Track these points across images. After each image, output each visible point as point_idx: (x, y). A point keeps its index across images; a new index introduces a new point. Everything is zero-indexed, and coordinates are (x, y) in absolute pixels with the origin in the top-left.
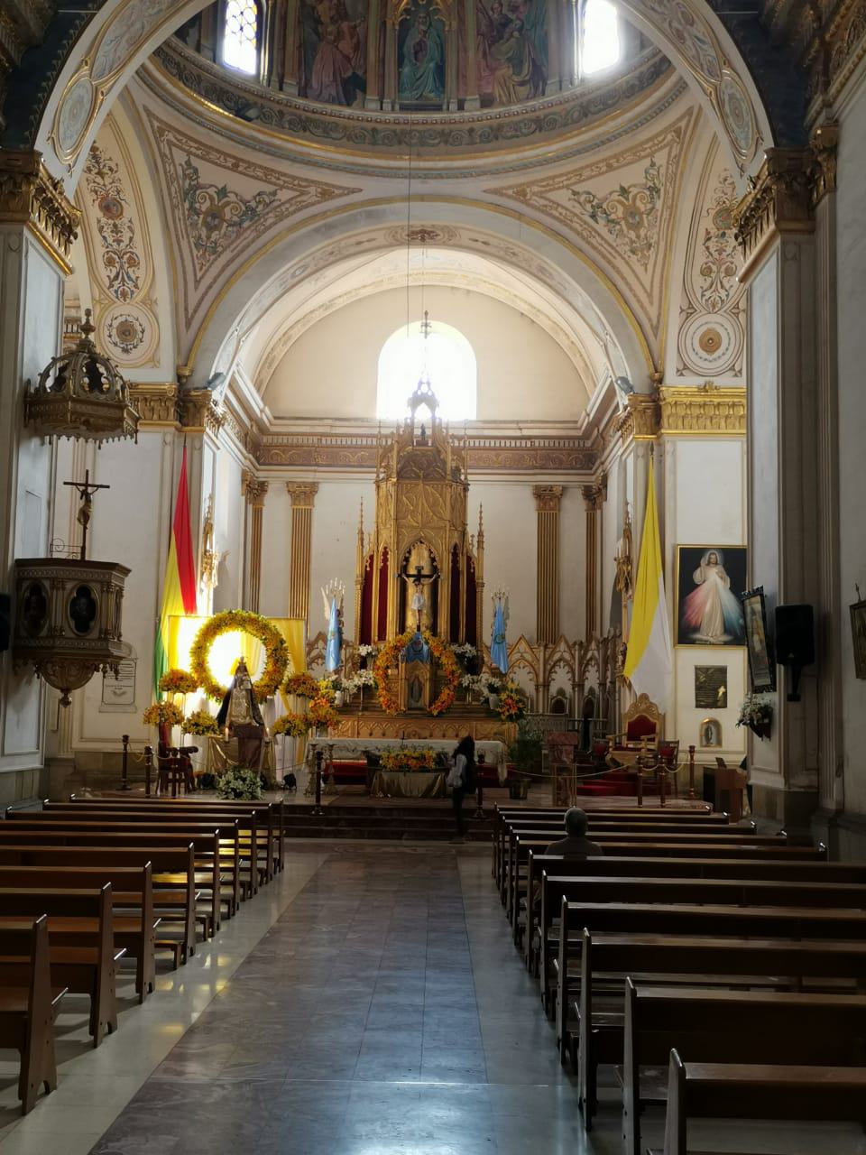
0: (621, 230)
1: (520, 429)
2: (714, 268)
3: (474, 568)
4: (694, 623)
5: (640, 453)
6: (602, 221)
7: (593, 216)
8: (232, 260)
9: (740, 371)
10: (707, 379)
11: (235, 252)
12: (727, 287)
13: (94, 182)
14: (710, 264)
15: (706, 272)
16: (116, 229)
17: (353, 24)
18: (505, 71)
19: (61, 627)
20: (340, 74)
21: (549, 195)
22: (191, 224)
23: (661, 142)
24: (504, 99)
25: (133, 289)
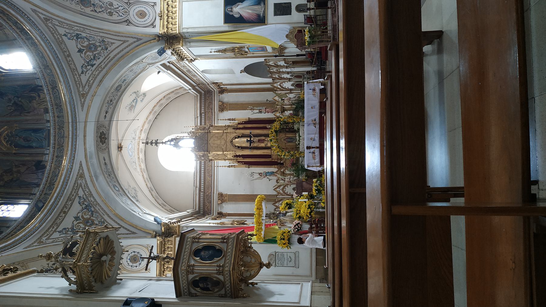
1: (197, 117)
2: (109, 10)
3: (243, 122)
5: (189, 44)
7: (92, 66)
8: (108, 215)
9: (155, 3)
10: (157, 15)
11: (104, 213)
12: (118, 6)
14: (107, 12)
15: (111, 14)
17: (14, 166)
18: (34, 104)
19: (217, 266)
20: (34, 171)
21: (84, 83)
23: (53, 30)
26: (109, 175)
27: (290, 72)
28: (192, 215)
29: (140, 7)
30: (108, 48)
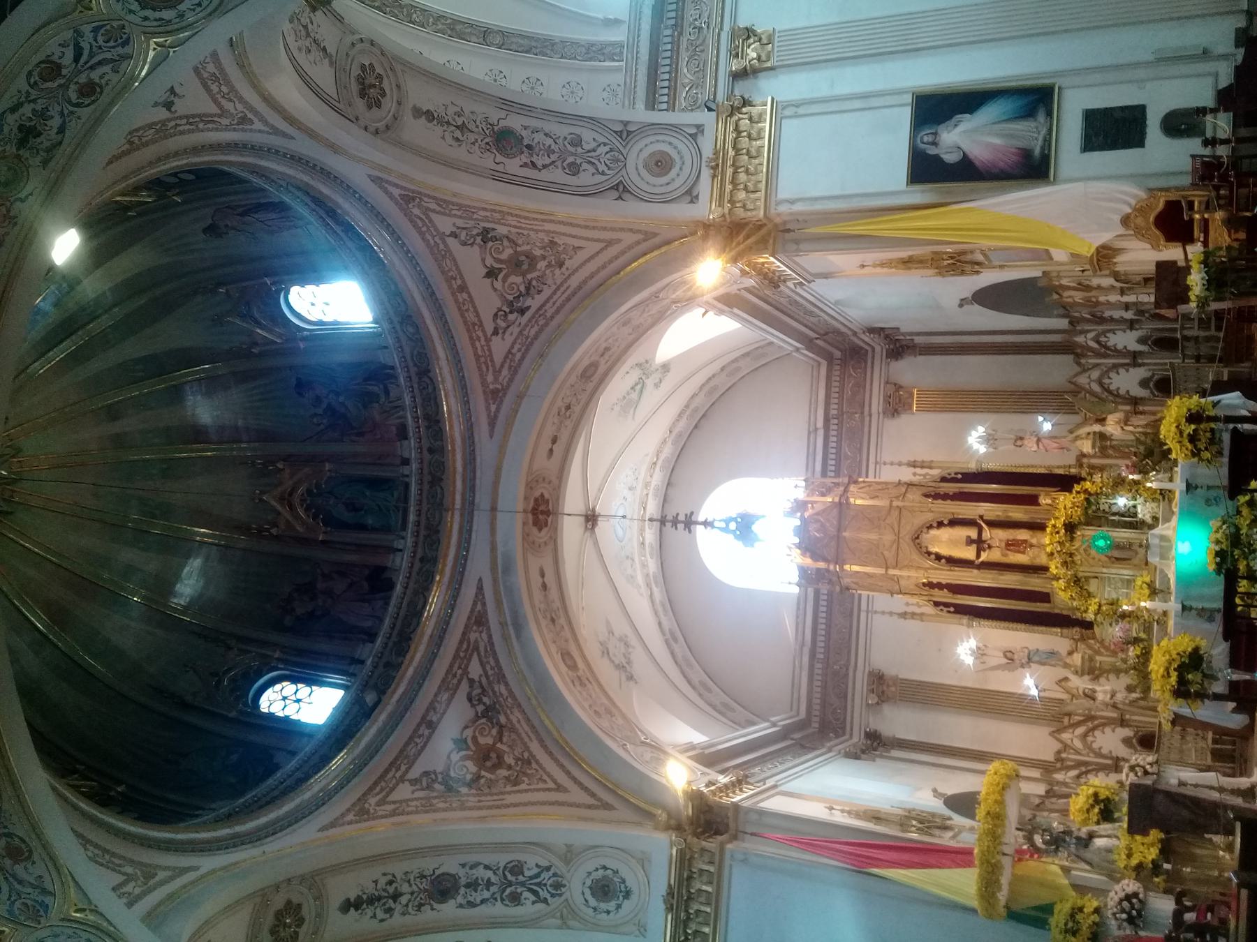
0: (538, 279)
1: (816, 429)
2: (571, 159)
3: (956, 474)
4: (1015, 158)
5: (795, 247)
6: (528, 302)
7: (522, 311)
8: (541, 741)
10: (704, 164)
13: (407, 905)
15: (574, 169)
16: (473, 885)
21: (498, 358)
22: (489, 787)
24: (401, 413)
25: (551, 873)
26: (553, 620)
27: (1135, 304)
28: (784, 734)
29: (658, 141)
30: (564, 263)
